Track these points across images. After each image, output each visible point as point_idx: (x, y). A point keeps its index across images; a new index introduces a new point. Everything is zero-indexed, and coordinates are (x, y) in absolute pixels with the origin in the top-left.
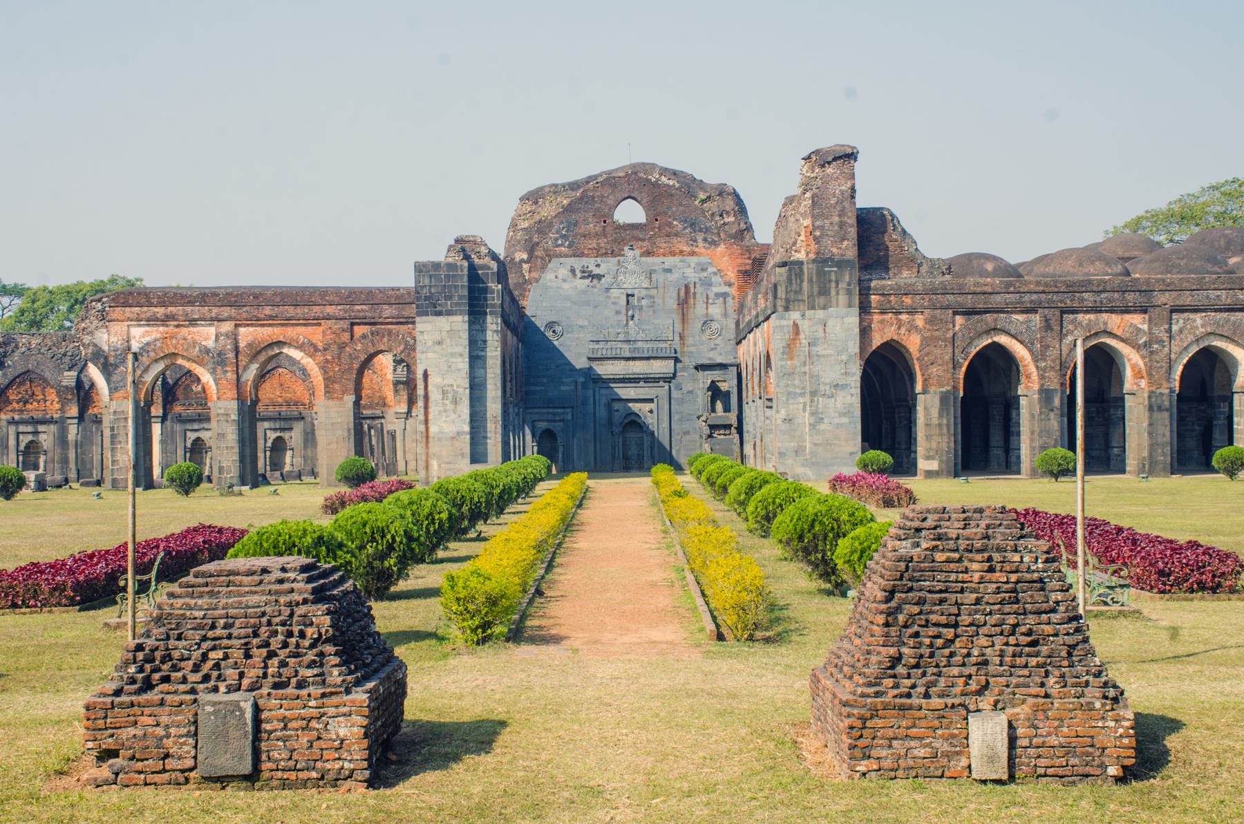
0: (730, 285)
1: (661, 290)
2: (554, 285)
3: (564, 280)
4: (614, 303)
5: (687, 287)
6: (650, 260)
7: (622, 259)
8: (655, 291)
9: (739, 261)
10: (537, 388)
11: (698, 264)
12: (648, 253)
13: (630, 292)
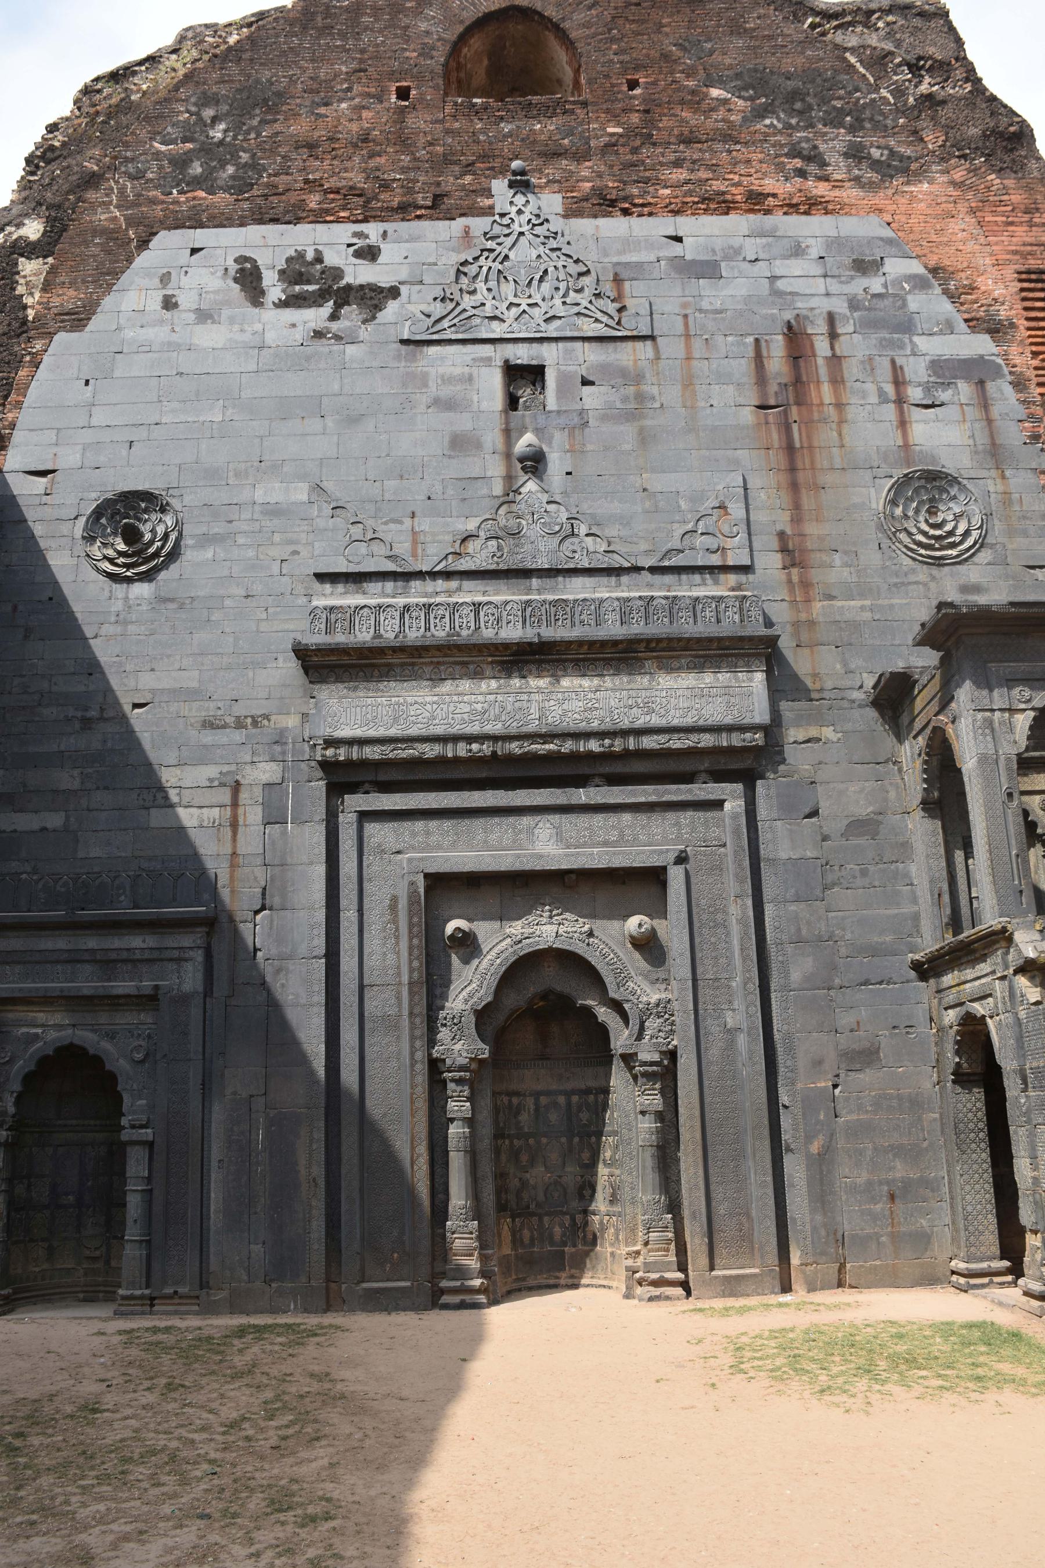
0: (996, 329)
1: (671, 348)
2: (158, 334)
3: (204, 316)
4: (447, 405)
5: (795, 336)
6: (613, 227)
7: (479, 224)
8: (645, 350)
9: (1021, 234)
10: (25, 822)
11: (835, 243)
12: (605, 204)
13: (522, 354)
